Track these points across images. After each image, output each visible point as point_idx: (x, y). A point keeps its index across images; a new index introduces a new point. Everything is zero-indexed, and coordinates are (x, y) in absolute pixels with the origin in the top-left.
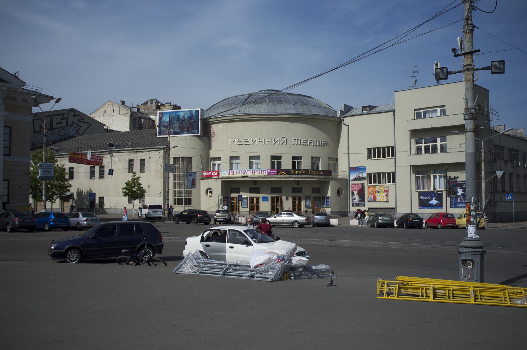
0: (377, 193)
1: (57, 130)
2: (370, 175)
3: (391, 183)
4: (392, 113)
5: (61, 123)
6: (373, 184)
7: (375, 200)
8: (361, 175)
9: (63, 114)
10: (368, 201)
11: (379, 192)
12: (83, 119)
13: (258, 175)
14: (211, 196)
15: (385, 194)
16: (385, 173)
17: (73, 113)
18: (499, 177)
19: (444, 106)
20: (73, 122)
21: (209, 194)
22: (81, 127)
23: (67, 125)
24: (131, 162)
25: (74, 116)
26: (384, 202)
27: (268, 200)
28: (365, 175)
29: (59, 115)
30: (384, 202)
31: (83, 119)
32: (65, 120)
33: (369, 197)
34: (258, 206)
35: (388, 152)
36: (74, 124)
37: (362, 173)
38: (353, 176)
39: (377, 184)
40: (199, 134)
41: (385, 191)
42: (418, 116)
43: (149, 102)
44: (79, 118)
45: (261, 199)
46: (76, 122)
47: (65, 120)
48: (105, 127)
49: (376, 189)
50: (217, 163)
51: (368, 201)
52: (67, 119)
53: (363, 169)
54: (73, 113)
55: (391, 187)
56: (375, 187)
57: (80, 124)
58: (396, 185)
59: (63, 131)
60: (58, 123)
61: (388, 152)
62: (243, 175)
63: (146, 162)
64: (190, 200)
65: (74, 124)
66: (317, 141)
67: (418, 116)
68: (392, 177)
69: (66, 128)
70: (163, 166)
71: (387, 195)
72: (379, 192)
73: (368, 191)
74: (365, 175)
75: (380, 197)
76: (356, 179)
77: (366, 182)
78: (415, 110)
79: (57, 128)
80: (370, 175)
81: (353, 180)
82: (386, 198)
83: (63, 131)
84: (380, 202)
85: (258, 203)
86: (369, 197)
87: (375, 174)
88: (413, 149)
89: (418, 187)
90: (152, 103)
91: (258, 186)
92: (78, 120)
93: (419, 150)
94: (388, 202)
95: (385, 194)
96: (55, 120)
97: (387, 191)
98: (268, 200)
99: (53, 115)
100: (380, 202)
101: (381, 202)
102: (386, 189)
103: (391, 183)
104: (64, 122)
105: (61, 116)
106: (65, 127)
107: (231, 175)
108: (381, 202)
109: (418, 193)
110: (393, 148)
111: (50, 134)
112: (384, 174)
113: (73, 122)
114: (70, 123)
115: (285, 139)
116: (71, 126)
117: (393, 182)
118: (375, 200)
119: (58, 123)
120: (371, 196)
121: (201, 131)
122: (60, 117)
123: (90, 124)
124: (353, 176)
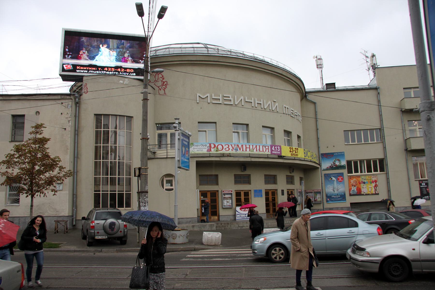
0: (362, 185)
2: (349, 163)
3: (379, 172)
4: (373, 92)
6: (354, 174)
7: (359, 193)
8: (337, 163)
10: (351, 195)
11: (364, 183)
13: (258, 152)
16: (363, 160)
21: (168, 186)
26: (372, 194)
28: (344, 163)
30: (372, 194)
33: (350, 190)
37: (339, 160)
38: (326, 164)
39: (359, 174)
41: (373, 182)
49: (361, 179)
51: (351, 195)
53: (341, 155)
55: (380, 176)
56: (359, 176)
58: (387, 174)
68: (381, 165)
70: (68, 129)
71: (376, 186)
72: (364, 183)
73: (350, 182)
74: (344, 163)
75: (367, 189)
76: (331, 168)
77: (345, 171)
81: (327, 169)
84: (366, 195)
87: (356, 163)
89: (416, 176)
94: (378, 194)
95: (374, 185)
97: (376, 181)
98: (262, 196)
100: (366, 195)
101: (368, 194)
102: (374, 179)
103: (379, 172)
107: (213, 151)
108: (368, 194)
109: (418, 182)
112: (361, 161)
115: (277, 104)
117: (382, 170)
118: (359, 193)
120: (354, 189)
124: (326, 164)
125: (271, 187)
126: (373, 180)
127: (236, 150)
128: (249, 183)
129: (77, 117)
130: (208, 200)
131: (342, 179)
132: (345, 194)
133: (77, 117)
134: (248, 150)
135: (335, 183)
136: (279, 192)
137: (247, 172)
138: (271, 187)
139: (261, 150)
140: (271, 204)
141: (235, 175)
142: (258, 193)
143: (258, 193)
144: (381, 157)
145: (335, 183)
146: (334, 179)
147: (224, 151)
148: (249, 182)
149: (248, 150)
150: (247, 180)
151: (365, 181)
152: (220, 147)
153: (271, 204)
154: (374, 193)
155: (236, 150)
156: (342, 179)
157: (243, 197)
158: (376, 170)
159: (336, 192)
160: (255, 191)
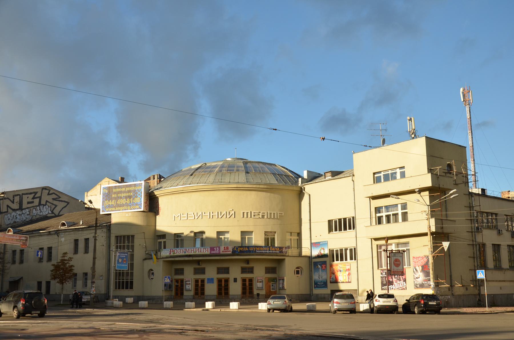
1: (27, 210)
5: (33, 202)
8: (322, 252)
9: (36, 193)
12: (60, 197)
13: (200, 253)
14: (152, 279)
15: (347, 273)
17: (47, 191)
19: (403, 168)
20: (47, 201)
22: (56, 206)
23: (40, 204)
24: (76, 241)
25: (49, 194)
26: (346, 282)
27: (213, 282)
29: (31, 193)
30: (346, 282)
31: (60, 197)
32: (38, 199)
33: (331, 277)
34: (203, 289)
35: (344, 224)
36: (48, 203)
37: (324, 249)
39: (339, 262)
40: (142, 210)
41: (347, 270)
42: (377, 180)
43: (152, 178)
44: (54, 196)
45: (206, 281)
46: (51, 201)
47: (38, 199)
48: (86, 206)
50: (162, 240)
51: (331, 282)
52: (40, 198)
53: (326, 243)
54: (47, 191)
57: (55, 202)
59: (34, 211)
60: (28, 203)
61: (344, 224)
62: (184, 254)
64: (132, 283)
65: (48, 203)
66: (271, 214)
67: (377, 180)
68: (354, 254)
69: (38, 208)
70: (105, 245)
71: (349, 274)
72: (340, 271)
78: (374, 174)
79: (28, 208)
80: (332, 251)
82: (349, 278)
83: (34, 211)
85: (203, 285)
86: (331, 277)
88: (374, 220)
90: (154, 179)
91: (203, 266)
92: (53, 199)
93: (379, 221)
94: (350, 282)
95: (347, 273)
96: (25, 200)
97: (349, 270)
98: (213, 282)
99: (23, 194)
102: (348, 267)
104: (37, 201)
105: (36, 196)
106: (37, 206)
107: (172, 254)
110: (353, 218)
111: (19, 215)
113: (47, 201)
114: (43, 202)
116: (44, 205)
119: (28, 203)
121: (145, 206)
122: (32, 196)
123: (68, 203)
125: (200, 277)
126: (347, 268)
127: (185, 252)
128: (204, 273)
129: (109, 237)
130: (179, 284)
131: (325, 267)
132: (327, 282)
133: (109, 237)
134: (192, 252)
135: (320, 270)
137: (203, 266)
138: (200, 277)
139: (202, 251)
140: (223, 289)
141: (195, 268)
142: (211, 281)
143: (211, 281)
145: (320, 270)
146: (319, 267)
147: (178, 254)
148: (204, 273)
149: (192, 252)
150: (202, 271)
151: (341, 269)
152: (176, 251)
153: (223, 289)
154: (347, 281)
155: (185, 252)
156: (325, 267)
157: (200, 283)
158: (337, 260)
159: (321, 279)
160: (208, 279)
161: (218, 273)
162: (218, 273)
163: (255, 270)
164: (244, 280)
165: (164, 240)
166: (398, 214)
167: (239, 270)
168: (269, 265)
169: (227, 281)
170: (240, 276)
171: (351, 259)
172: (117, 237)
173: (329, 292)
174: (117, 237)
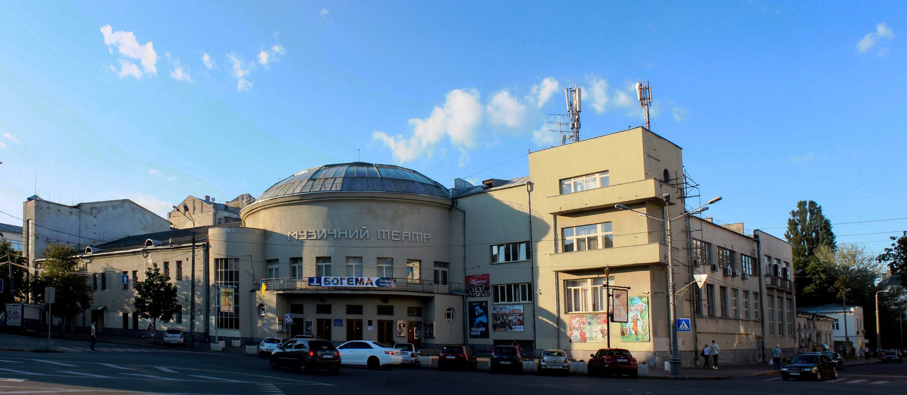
6: (500, 302)
18: (700, 285)
39: (506, 302)
63: (183, 266)
91: (328, 303)
136: (365, 323)
142: (339, 322)
144: (530, 281)
148: (329, 312)
150: (327, 309)
160: (336, 320)
161: (348, 313)
162: (348, 313)
163: (395, 311)
164: (381, 323)
165: (277, 266)
166: (595, 238)
167: (375, 310)
168: (414, 304)
169: (360, 323)
170: (376, 318)
171: (524, 299)
172: (217, 260)
173: (492, 343)
174: (217, 260)
